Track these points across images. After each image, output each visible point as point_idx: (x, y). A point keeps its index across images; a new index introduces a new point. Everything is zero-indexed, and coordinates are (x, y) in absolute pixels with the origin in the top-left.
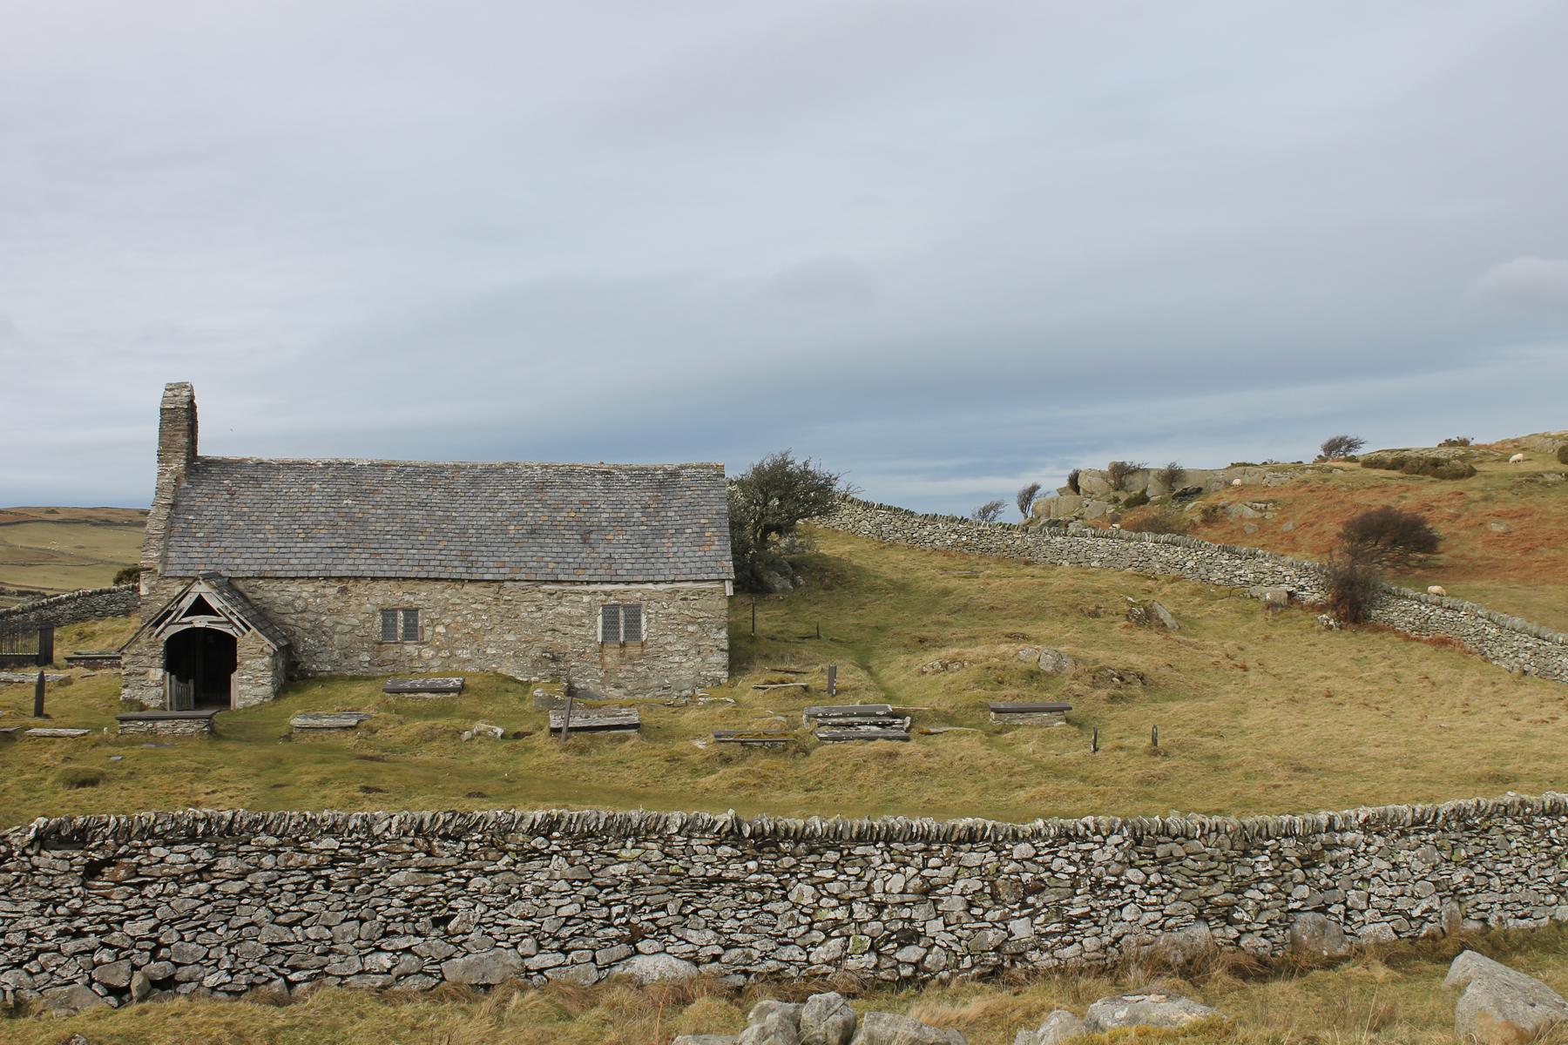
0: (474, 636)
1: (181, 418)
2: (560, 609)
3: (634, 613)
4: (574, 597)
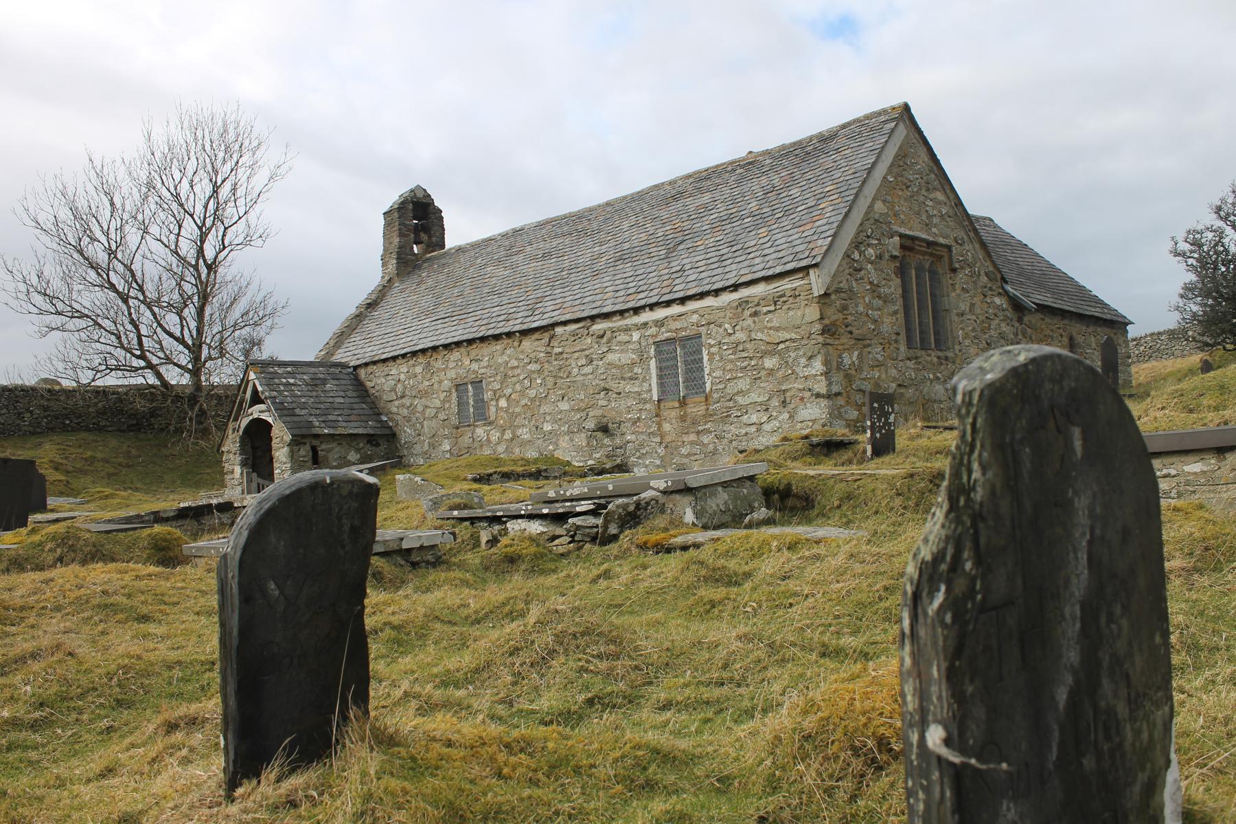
0: (531, 409)
1: (416, 221)
2: (611, 357)
3: (691, 343)
4: (623, 337)
